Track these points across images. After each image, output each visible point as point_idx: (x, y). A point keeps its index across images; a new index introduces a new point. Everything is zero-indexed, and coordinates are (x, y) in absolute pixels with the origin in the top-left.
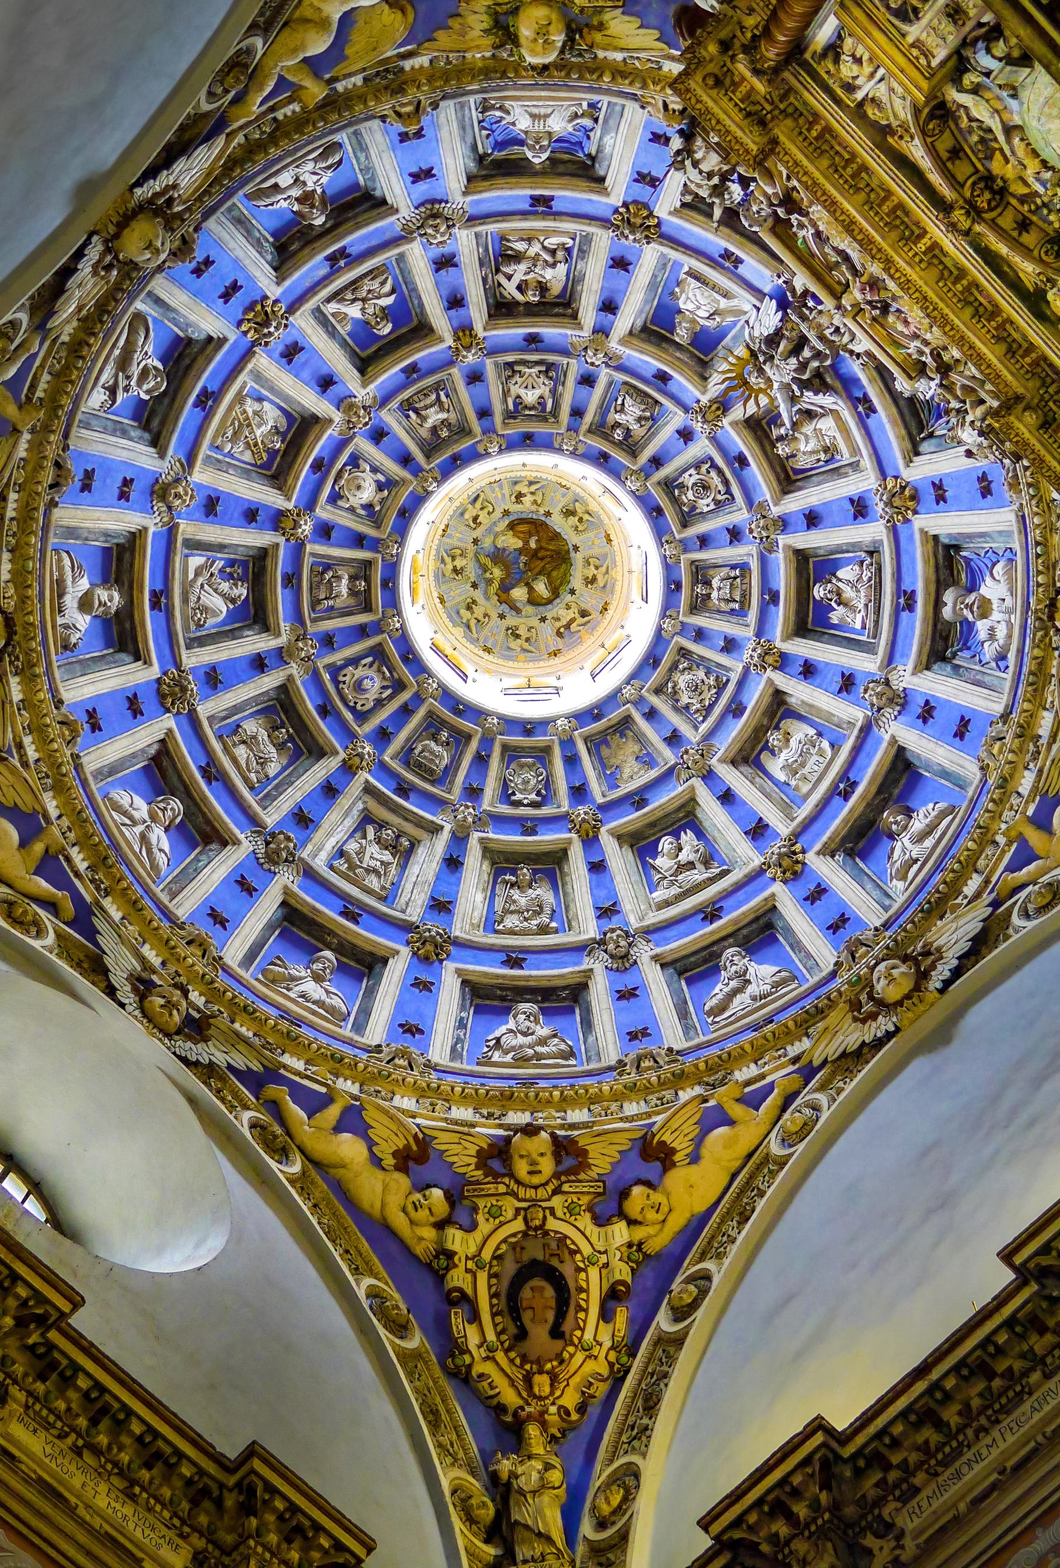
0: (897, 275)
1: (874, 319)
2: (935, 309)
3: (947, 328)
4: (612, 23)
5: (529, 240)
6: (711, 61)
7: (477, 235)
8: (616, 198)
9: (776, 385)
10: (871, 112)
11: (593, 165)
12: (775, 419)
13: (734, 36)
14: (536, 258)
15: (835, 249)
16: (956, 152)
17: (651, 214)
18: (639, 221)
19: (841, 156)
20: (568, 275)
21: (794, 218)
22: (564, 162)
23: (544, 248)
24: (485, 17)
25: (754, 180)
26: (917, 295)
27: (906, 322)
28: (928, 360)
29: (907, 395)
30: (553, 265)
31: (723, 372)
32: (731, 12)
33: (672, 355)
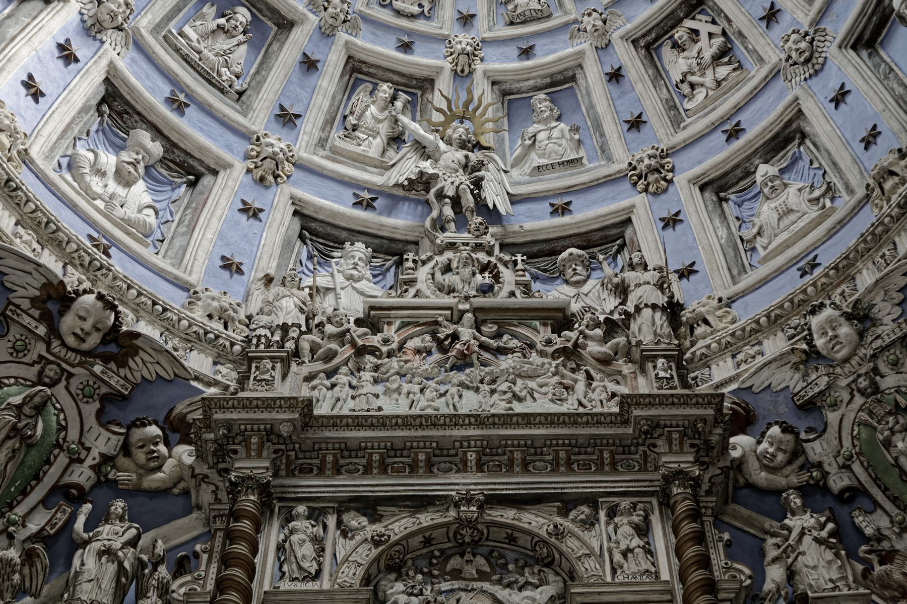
0: (467, 421)
1: (437, 323)
2: (421, 425)
3: (400, 421)
4: (790, 374)
5: (719, 83)
6: (710, 432)
7: (761, 60)
8: (681, 179)
9: (442, 146)
10: (585, 509)
11: (717, 194)
12: (411, 106)
13: (707, 455)
14: (703, 71)
15: (512, 351)
16: (511, 540)
17: (646, 190)
18: (651, 178)
19: (575, 454)
20: (667, 73)
21: (559, 342)
22: (741, 179)
23: (702, 85)
24: (880, 316)
25: (605, 339)
26: (442, 422)
27: (418, 351)
28: (375, 340)
29: (347, 245)
30: (685, 75)
31: (486, 109)
32: (721, 464)
33: (534, 78)
